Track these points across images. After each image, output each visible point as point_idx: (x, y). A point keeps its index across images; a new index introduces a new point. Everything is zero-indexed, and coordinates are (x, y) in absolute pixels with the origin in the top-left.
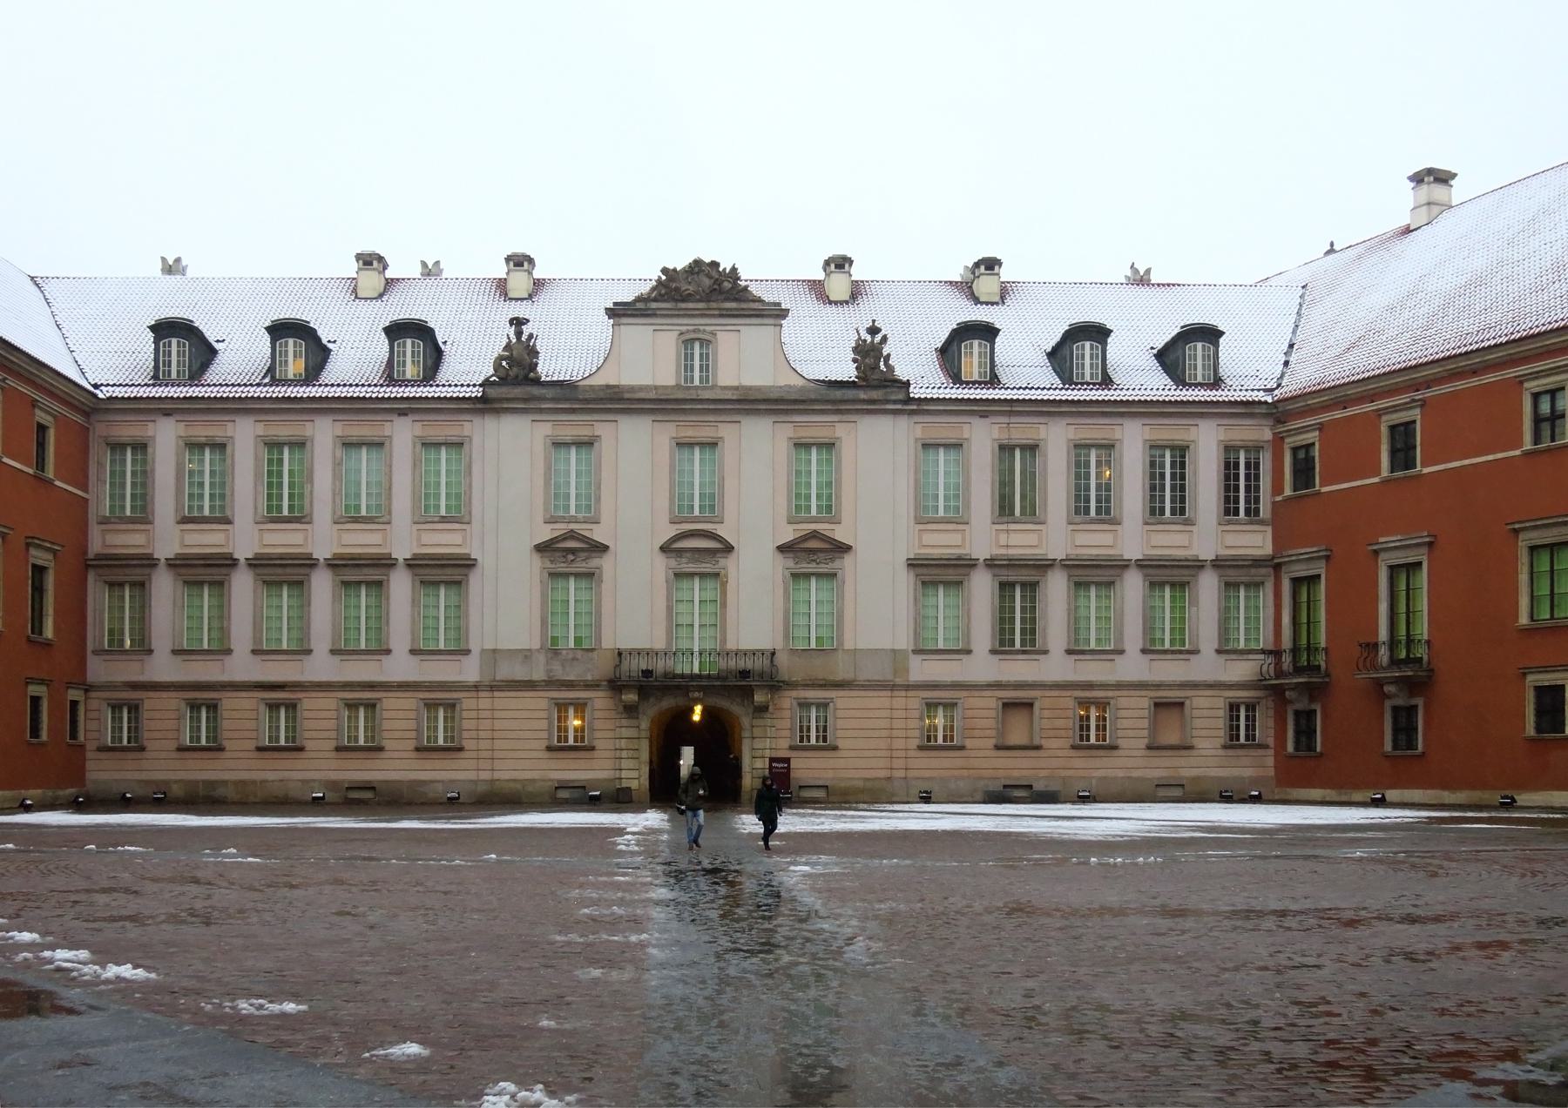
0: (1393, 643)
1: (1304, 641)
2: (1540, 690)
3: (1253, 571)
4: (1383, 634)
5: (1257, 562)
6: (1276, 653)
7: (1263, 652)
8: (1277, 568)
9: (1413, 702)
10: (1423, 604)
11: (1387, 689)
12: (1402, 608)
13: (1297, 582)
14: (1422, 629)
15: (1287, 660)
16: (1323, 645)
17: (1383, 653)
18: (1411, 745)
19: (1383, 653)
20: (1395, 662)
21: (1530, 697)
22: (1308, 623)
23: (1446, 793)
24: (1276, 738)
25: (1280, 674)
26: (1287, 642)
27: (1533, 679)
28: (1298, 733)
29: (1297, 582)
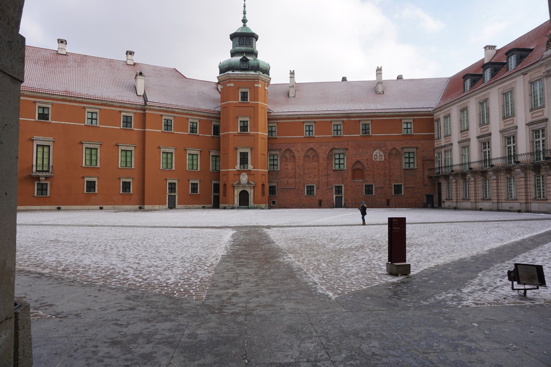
17: (34, 168)
19: (34, 168)
20: (37, 171)
21: (85, 183)
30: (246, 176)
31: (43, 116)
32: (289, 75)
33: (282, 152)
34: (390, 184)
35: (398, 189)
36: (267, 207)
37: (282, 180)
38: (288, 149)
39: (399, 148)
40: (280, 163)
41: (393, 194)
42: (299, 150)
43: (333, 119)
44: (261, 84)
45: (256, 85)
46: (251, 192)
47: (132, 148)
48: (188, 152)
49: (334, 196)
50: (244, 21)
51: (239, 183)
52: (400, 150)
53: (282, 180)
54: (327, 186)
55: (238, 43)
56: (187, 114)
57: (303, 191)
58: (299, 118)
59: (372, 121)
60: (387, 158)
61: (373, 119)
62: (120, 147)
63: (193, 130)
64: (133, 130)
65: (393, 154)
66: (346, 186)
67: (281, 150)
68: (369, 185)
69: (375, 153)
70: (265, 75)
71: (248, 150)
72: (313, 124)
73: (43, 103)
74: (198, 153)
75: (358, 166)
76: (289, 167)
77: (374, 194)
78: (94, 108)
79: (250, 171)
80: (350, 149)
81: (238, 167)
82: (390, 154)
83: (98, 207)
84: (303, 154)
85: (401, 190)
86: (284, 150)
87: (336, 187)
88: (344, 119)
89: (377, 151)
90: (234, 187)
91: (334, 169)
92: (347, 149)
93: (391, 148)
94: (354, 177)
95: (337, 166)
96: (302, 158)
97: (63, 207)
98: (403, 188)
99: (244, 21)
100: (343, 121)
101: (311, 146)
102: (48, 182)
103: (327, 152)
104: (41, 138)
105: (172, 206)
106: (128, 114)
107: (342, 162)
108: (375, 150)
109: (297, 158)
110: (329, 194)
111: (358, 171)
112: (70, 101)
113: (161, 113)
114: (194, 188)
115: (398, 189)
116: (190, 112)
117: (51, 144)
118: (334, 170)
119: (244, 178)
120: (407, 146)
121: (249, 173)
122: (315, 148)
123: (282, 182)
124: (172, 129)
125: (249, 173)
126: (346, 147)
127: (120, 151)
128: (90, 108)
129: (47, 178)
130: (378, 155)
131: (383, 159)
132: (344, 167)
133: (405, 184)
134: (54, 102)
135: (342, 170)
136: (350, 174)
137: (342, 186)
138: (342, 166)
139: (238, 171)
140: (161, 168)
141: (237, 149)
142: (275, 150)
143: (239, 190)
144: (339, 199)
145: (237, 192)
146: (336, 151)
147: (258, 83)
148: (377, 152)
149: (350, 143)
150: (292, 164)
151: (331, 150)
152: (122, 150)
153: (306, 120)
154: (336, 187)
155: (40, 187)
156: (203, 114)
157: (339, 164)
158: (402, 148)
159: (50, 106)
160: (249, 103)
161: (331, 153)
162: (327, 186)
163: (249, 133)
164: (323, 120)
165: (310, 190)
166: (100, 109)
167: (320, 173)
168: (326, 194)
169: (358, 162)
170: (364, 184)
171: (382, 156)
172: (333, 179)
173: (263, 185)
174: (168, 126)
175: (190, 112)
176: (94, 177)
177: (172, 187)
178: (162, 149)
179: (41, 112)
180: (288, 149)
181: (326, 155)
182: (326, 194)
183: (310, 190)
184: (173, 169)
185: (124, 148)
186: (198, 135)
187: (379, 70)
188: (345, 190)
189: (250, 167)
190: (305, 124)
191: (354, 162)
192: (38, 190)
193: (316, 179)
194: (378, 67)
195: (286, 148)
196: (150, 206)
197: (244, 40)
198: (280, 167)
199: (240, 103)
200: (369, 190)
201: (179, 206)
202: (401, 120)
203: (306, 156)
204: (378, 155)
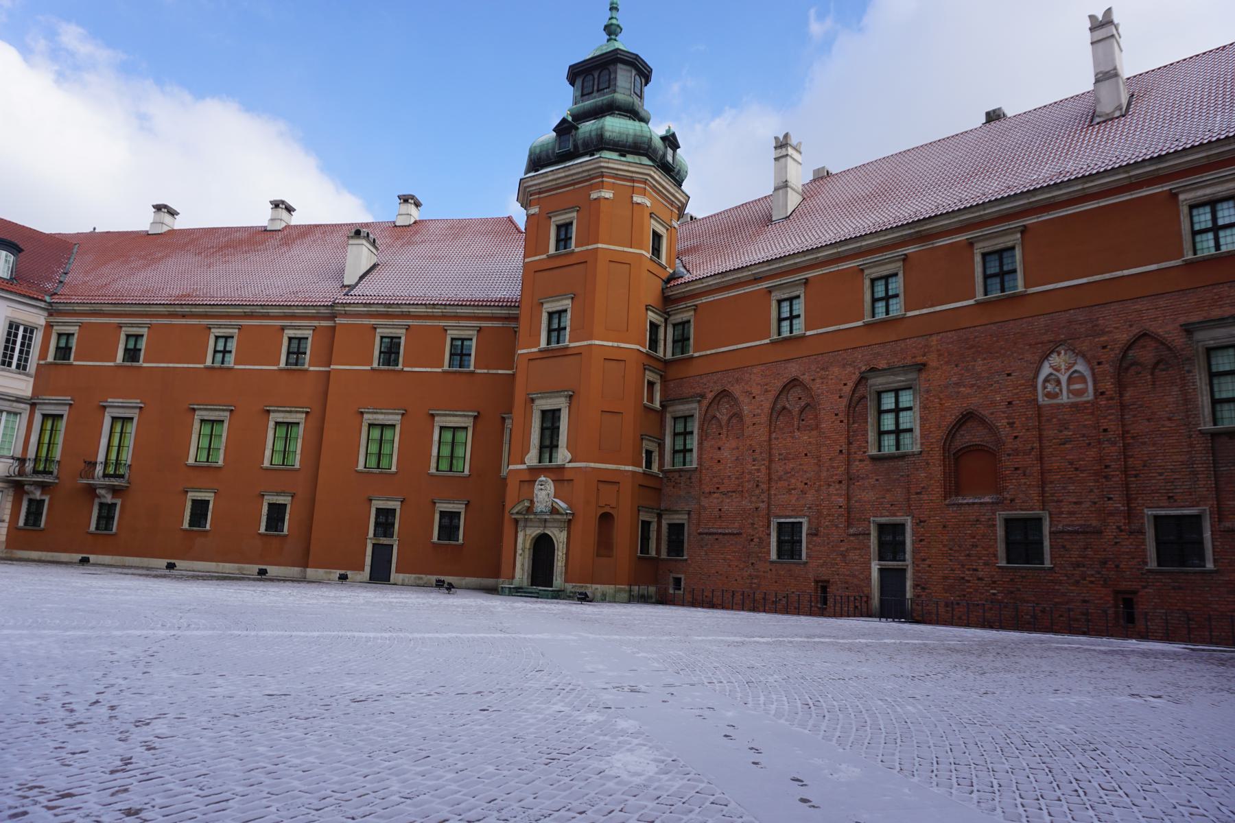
0: (106, 464)
1: (44, 454)
2: (194, 501)
3: (15, 404)
4: (101, 457)
5: (19, 400)
6: (22, 461)
7: (13, 458)
8: (33, 405)
9: (114, 501)
10: (130, 441)
11: (98, 491)
12: (116, 442)
13: (45, 416)
14: (127, 456)
15: (29, 466)
16: (58, 458)
17: (99, 470)
18: (108, 527)
19: (99, 470)
20: (105, 475)
21: (189, 505)
22: (49, 444)
23: (118, 558)
24: (11, 515)
25: (21, 473)
26: (31, 453)
27: (192, 495)
28: (28, 513)
29: (45, 416)
30: (551, 487)
31: (132, 354)
32: (773, 154)
33: (705, 402)
34: (1130, 514)
35: (1178, 540)
36: (626, 595)
37: (705, 502)
38: (724, 394)
39: (1169, 330)
40: (700, 444)
41: (1152, 564)
42: (755, 391)
43: (870, 259)
44: (612, 187)
45: (594, 195)
46: (560, 537)
47: (300, 418)
48: (439, 421)
49: (875, 567)
50: (611, 31)
51: (529, 510)
52: (1178, 340)
53: (705, 502)
54: (849, 525)
55: (579, 93)
56: (444, 317)
57: (763, 543)
58: (757, 279)
59: (1024, 230)
60: (1108, 385)
61: (1030, 221)
62: (272, 415)
63: (460, 354)
64: (307, 370)
65: (1135, 366)
66: (920, 522)
67: (703, 396)
68: (1025, 520)
69: (1046, 370)
70: (630, 158)
71: (560, 403)
72: (800, 291)
73: (132, 325)
74: (469, 422)
75: (972, 436)
76: (725, 453)
77: (1048, 564)
78: (227, 327)
79: (561, 468)
80: (933, 364)
81: (532, 459)
82: (1124, 367)
83: (163, 563)
84: (767, 406)
85: (1201, 543)
86: (710, 396)
87: (882, 528)
88: (910, 250)
89: (1055, 359)
90: (516, 521)
91: (873, 451)
92: (921, 367)
93: (1123, 337)
94: (954, 485)
95: (889, 442)
96: (764, 419)
97: (92, 558)
98: (1207, 535)
99: (611, 31)
100: (905, 259)
101: (793, 370)
102: (119, 502)
103: (847, 390)
104: (118, 401)
105: (380, 576)
106: (299, 333)
107: (906, 420)
108: (1046, 357)
109: (748, 420)
110: (853, 556)
111: (967, 456)
112: (184, 316)
113: (373, 321)
114: (449, 524)
115: (1178, 540)
116: (449, 310)
117: (134, 414)
118: (874, 459)
119: (544, 494)
120: (1216, 313)
121: (558, 474)
122: (806, 378)
123: (705, 508)
124: (401, 360)
125: (558, 474)
126: (920, 359)
127: (271, 424)
128: (220, 327)
129: (115, 491)
130: (1063, 377)
131: (1090, 395)
132: (911, 444)
133: (1220, 514)
134: (154, 321)
135: (903, 457)
136: (937, 471)
137: (903, 526)
138: (906, 439)
139: (531, 470)
140: (361, 467)
141: (533, 400)
142: (684, 400)
143: (529, 531)
144: (891, 578)
145: (525, 539)
146: (878, 382)
147: (601, 186)
148: (1057, 365)
149: (934, 340)
150: (734, 443)
151: (862, 379)
152: (277, 423)
153: (777, 282)
154: (882, 528)
155: (105, 512)
156: (487, 311)
157: (898, 432)
158: (1188, 330)
159: (144, 331)
160: (572, 252)
161: (861, 390)
162: (849, 525)
163: (566, 348)
164: (834, 268)
165: (789, 538)
166: (240, 328)
167: (824, 474)
168: (844, 556)
169: (967, 417)
170: (1000, 515)
171: (1083, 379)
172: (870, 496)
173: (606, 519)
174: (391, 351)
175: (449, 310)
176: (206, 490)
177: (385, 520)
178: (366, 416)
179: (131, 346)
180: (724, 394)
181: (845, 402)
182: (844, 556)
183: (789, 538)
184: (394, 469)
185: (280, 417)
186: (472, 373)
187: (1103, 27)
188: (919, 540)
189: (563, 455)
190: (776, 295)
191: (951, 419)
192: (99, 518)
193: (810, 496)
194: (1092, 17)
195: (720, 388)
196: (321, 571)
197: (605, 77)
198: (700, 458)
199: (550, 257)
200: (1023, 539)
201: (401, 576)
202: (1173, 196)
203: (778, 411)
204: (1063, 377)
